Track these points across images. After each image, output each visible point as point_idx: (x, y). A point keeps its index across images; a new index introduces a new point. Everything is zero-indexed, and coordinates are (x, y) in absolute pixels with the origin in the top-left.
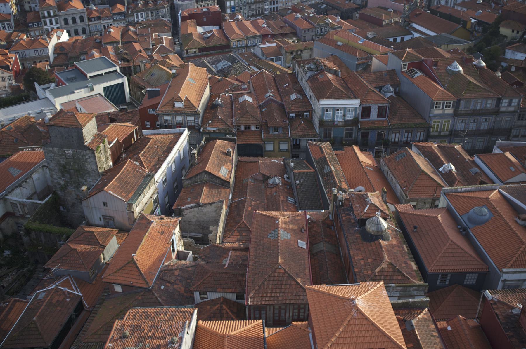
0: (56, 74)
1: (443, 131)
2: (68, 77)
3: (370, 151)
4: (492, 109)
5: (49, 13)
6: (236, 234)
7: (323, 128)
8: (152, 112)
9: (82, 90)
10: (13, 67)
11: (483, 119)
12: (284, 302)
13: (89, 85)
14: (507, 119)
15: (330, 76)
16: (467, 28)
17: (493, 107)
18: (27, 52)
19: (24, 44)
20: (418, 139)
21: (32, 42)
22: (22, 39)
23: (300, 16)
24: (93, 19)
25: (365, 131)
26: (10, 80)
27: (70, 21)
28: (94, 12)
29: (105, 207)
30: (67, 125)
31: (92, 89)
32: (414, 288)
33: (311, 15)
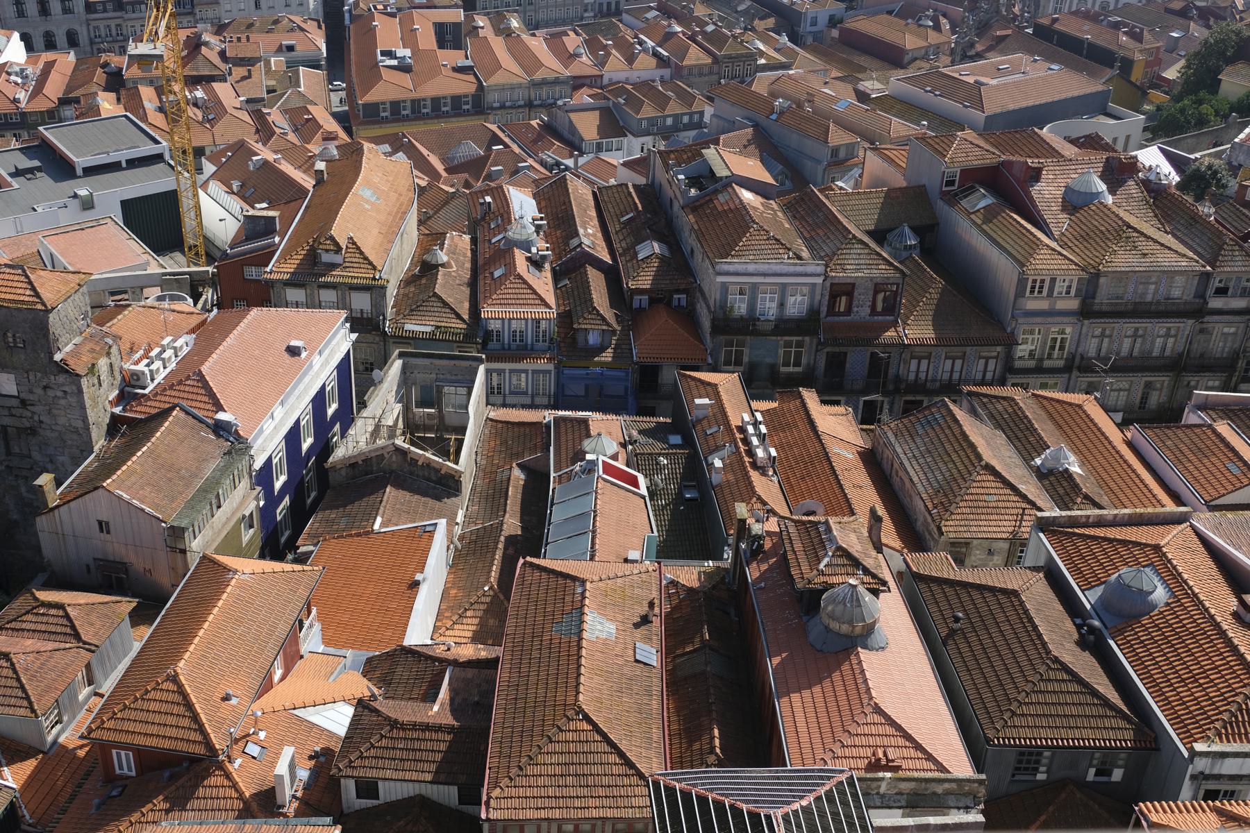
1: (1050, 357)
3: (847, 404)
4: (1186, 303)
6: (469, 621)
7: (722, 338)
8: (252, 272)
11: (1159, 327)
12: (587, 814)
14: (1226, 330)
15: (747, 196)
16: (1133, 79)
17: (1189, 296)
20: (979, 376)
23: (679, 29)
25: (837, 350)
29: (104, 536)
32: (947, 786)
33: (710, 28)
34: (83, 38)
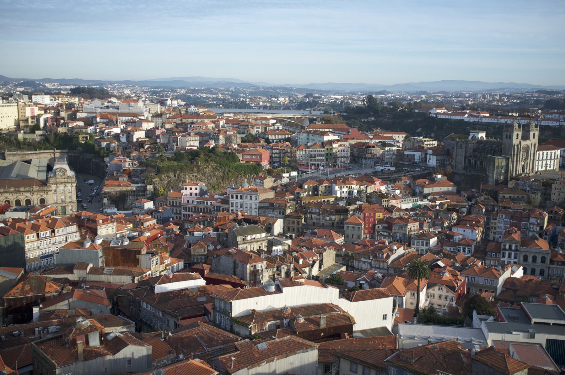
0: (499, 308)
2: (511, 315)
5: (510, 247)
9: (521, 334)
10: (459, 289)
13: (531, 331)
18: (477, 278)
19: (477, 270)
21: (484, 271)
22: (476, 265)
24: (556, 263)
26: (452, 300)
27: (530, 259)
28: (559, 256)
30: (494, 365)
31: (533, 337)
34: (546, 273)
